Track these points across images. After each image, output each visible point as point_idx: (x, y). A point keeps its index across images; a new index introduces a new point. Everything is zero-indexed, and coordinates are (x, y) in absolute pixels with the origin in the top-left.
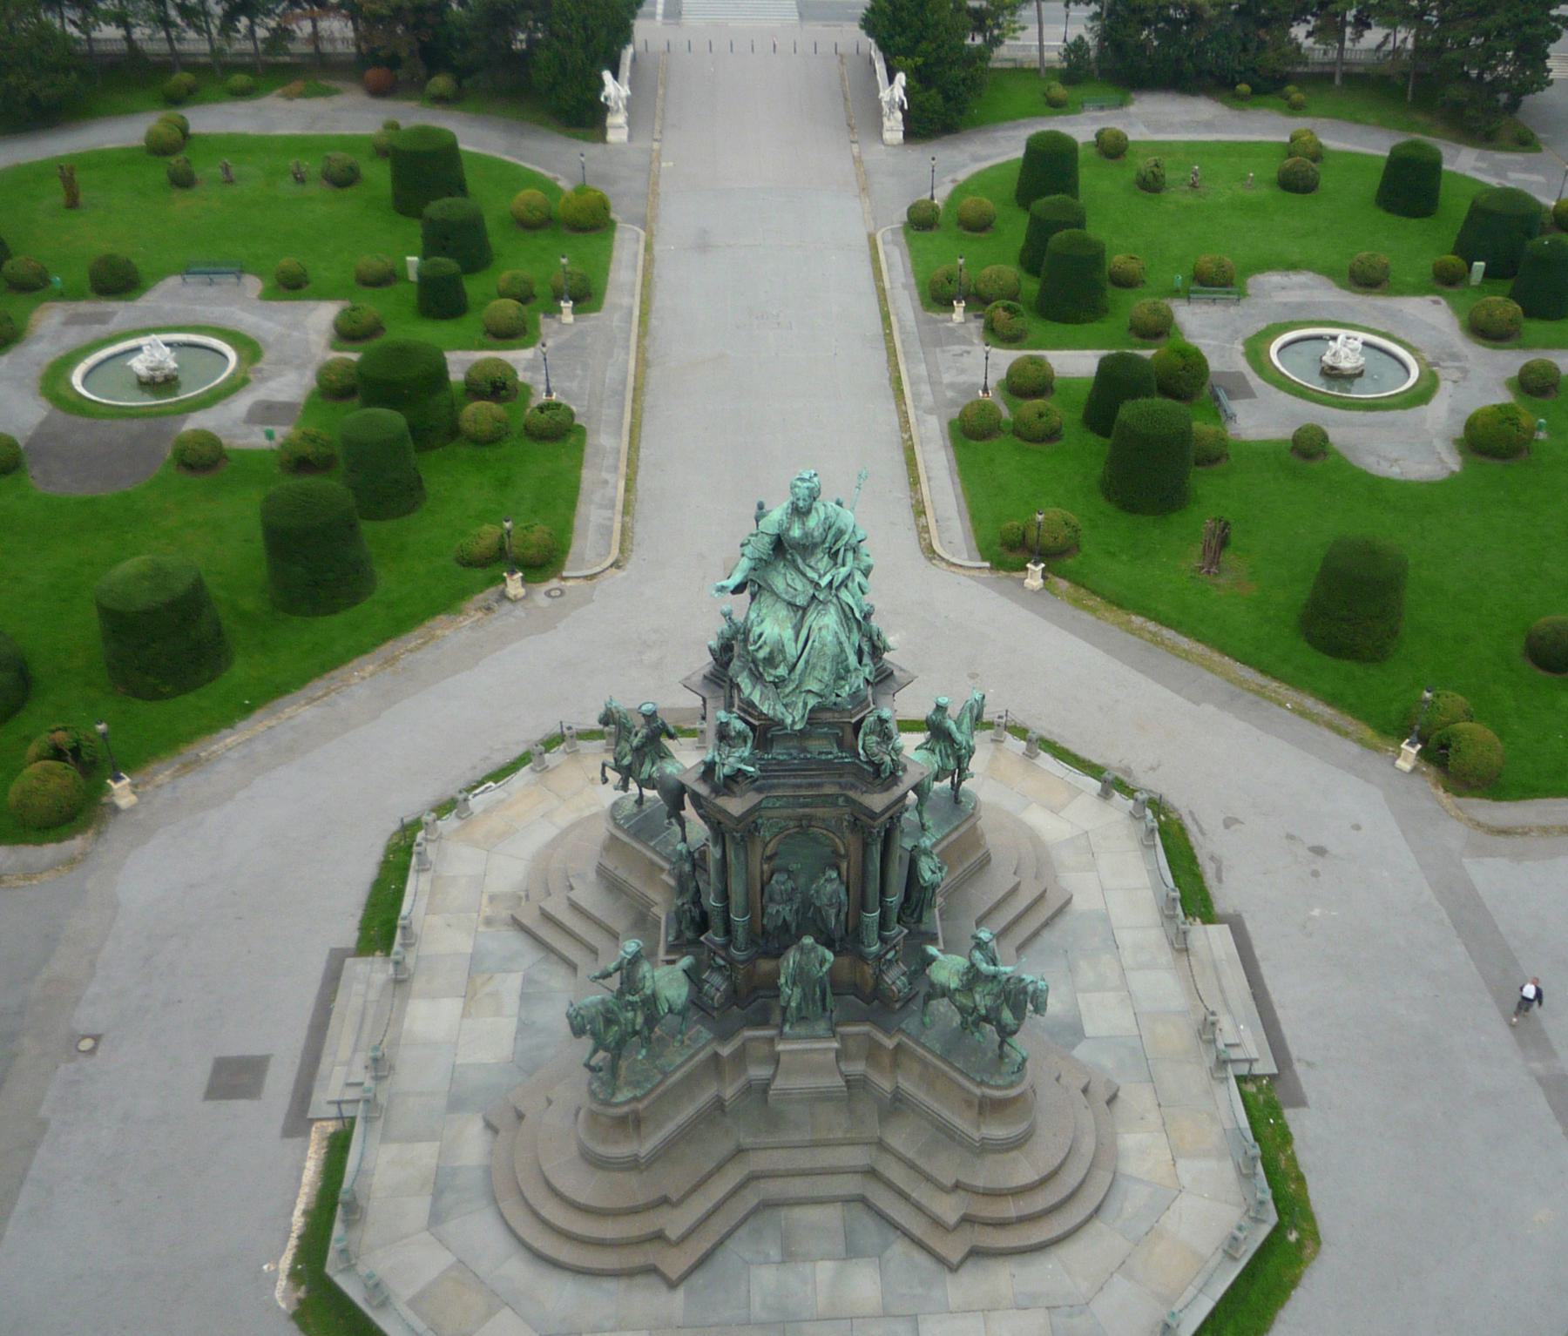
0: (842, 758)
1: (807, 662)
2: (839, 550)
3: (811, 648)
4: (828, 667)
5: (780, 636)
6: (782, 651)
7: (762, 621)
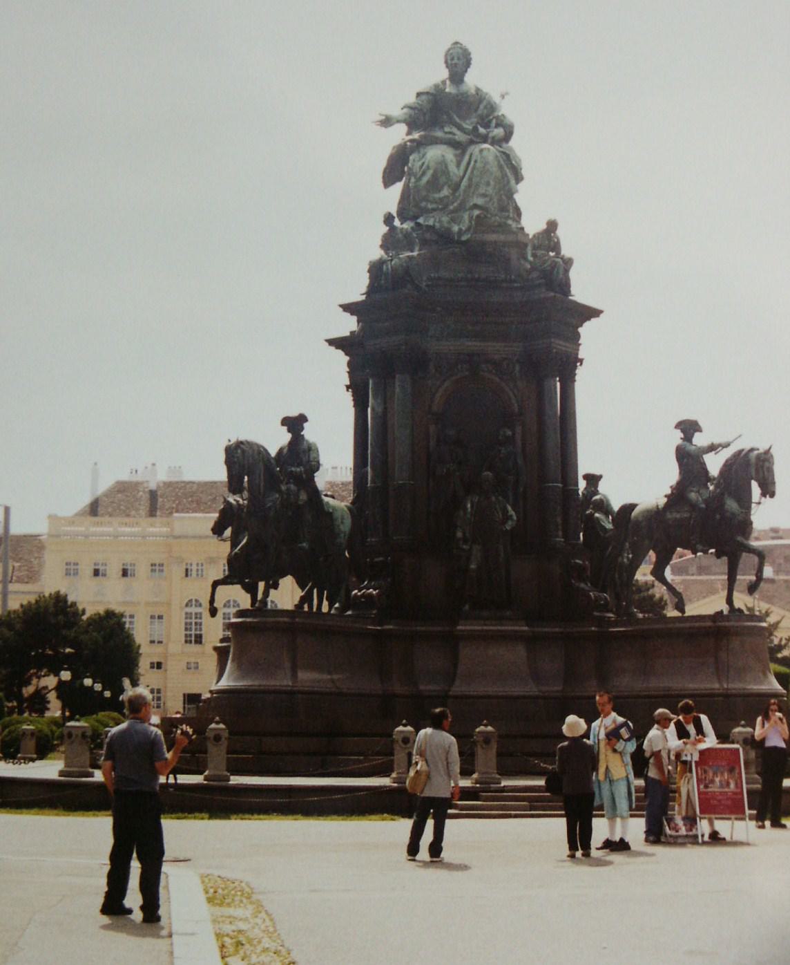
0: (511, 281)
1: (470, 179)
2: (491, 120)
3: (474, 168)
4: (492, 183)
5: (443, 156)
6: (446, 172)
7: (424, 156)
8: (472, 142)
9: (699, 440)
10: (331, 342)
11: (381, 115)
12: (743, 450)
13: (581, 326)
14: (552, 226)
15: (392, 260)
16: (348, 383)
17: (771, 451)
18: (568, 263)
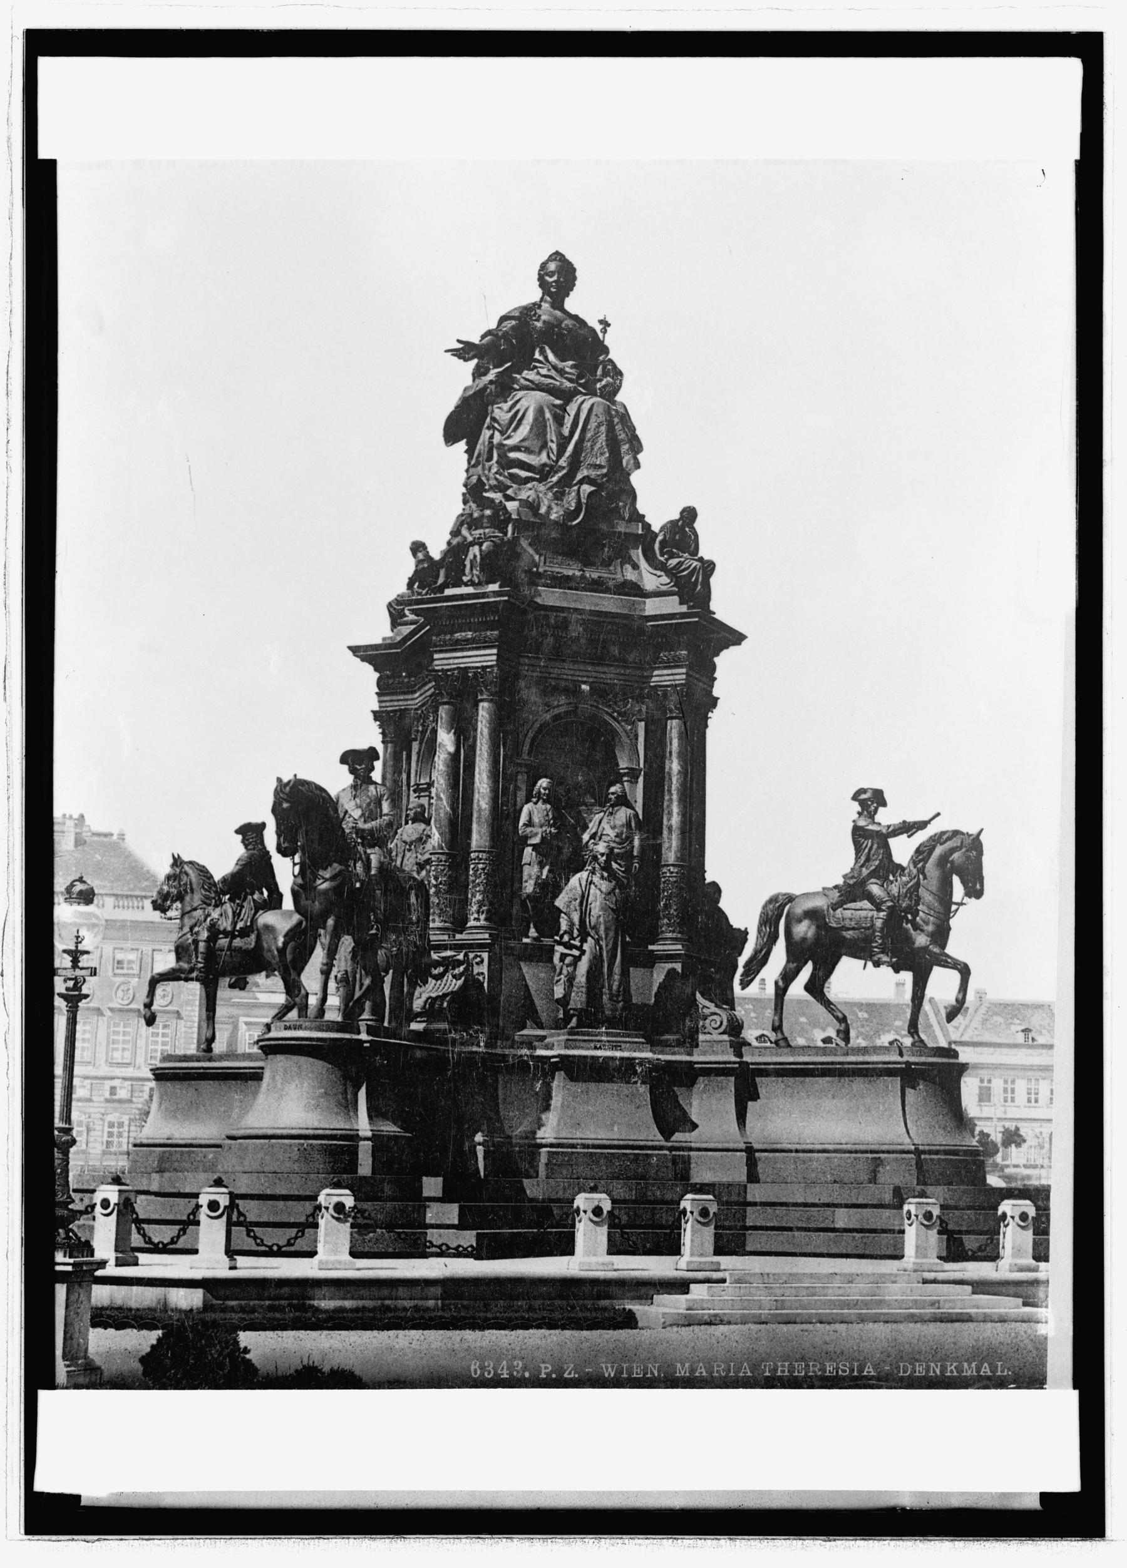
8: (577, 393)
9: (886, 817)
10: (355, 650)
11: (459, 341)
12: (943, 833)
13: (718, 655)
14: (689, 515)
15: (481, 545)
16: (376, 708)
17: (982, 838)
18: (709, 567)
